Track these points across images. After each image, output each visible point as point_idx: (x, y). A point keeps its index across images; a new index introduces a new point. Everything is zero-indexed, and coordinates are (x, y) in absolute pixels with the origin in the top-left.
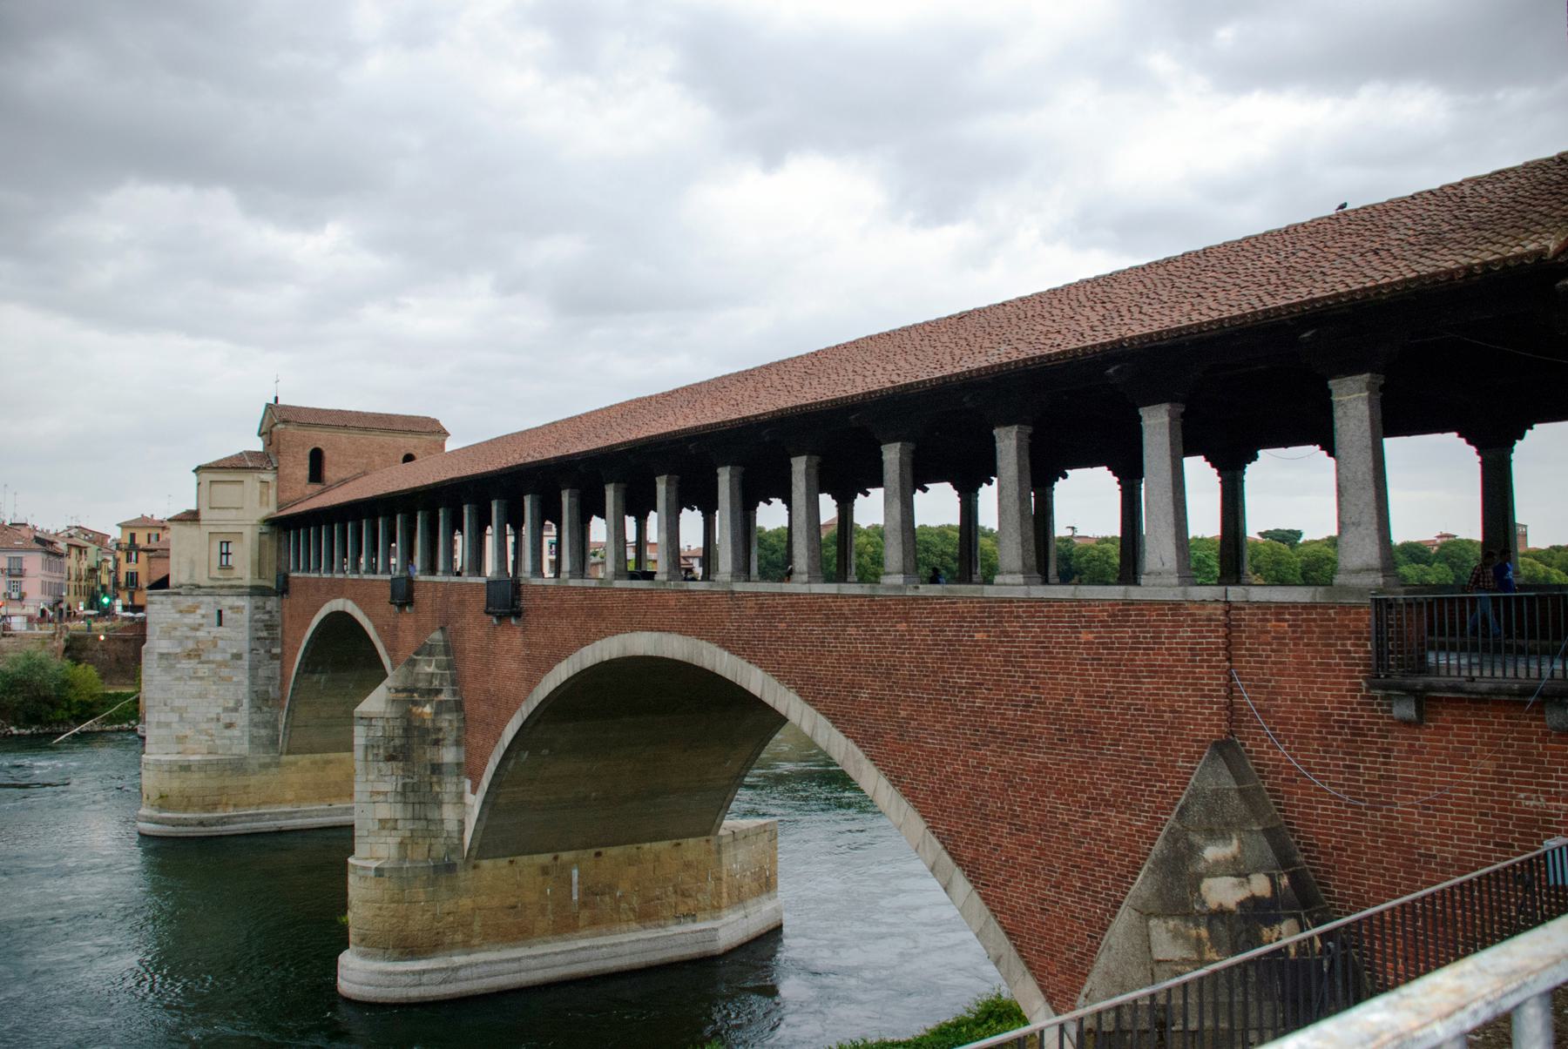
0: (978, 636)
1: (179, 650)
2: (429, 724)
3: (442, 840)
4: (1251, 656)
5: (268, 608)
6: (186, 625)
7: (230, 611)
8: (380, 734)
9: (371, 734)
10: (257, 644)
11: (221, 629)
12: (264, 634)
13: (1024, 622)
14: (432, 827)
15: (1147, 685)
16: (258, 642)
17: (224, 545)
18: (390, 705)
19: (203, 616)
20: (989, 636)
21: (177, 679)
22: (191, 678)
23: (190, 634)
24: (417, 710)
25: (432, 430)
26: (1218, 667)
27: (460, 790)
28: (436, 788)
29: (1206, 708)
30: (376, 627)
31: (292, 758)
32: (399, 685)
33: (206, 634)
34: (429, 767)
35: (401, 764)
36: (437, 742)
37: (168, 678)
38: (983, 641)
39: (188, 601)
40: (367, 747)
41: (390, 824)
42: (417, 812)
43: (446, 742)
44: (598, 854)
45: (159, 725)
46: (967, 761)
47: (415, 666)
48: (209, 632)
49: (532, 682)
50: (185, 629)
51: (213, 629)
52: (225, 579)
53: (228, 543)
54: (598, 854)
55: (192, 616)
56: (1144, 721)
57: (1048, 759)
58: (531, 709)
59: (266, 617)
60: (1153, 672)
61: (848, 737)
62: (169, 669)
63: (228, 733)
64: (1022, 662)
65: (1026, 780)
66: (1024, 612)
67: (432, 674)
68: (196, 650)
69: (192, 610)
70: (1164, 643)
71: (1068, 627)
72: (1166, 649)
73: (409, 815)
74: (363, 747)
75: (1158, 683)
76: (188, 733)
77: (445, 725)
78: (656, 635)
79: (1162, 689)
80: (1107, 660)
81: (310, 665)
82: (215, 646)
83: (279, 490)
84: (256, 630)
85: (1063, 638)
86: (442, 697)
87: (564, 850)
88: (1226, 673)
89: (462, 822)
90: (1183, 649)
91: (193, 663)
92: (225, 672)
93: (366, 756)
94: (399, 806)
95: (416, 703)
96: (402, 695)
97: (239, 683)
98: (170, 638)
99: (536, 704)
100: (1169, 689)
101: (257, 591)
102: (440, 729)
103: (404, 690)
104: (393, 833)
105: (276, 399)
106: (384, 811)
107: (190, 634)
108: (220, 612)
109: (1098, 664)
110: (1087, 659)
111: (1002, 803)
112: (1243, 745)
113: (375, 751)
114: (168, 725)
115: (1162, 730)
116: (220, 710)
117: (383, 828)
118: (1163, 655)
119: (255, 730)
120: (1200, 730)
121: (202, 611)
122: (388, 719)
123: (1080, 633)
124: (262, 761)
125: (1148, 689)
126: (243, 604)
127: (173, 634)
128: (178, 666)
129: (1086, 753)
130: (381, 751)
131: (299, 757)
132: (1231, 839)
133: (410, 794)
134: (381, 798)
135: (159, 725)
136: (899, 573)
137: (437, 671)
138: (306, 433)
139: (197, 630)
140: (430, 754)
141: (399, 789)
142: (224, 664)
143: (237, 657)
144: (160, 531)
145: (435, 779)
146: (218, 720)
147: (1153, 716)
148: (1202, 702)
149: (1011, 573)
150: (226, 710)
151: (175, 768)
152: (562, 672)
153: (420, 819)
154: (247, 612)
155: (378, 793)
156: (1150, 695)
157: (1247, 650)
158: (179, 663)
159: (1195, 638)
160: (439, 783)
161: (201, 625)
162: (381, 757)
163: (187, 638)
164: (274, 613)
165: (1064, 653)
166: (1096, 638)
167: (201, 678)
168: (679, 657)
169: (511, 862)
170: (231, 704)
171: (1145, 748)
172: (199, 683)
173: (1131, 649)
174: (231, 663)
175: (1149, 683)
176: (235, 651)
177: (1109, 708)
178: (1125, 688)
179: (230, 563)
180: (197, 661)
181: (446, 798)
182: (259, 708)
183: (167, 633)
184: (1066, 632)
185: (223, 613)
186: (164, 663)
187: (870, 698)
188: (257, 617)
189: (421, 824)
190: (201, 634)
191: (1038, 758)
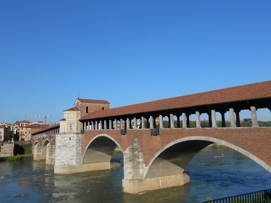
1: (62, 145)
2: (137, 155)
12: (78, 141)
19: (67, 139)
21: (62, 151)
24: (135, 152)
28: (138, 166)
30: (115, 139)
31: (83, 165)
32: (131, 148)
36: (138, 158)
39: (64, 135)
44: (164, 178)
54: (164, 178)
55: (65, 139)
58: (163, 151)
59: (79, 138)
63: (71, 161)
67: (136, 146)
73: (134, 171)
77: (140, 154)
81: (90, 147)
83: (81, 114)
86: (139, 150)
87: (159, 177)
91: (65, 147)
92: (71, 149)
94: (132, 169)
95: (134, 151)
96: (132, 150)
97: (74, 151)
99: (164, 150)
101: (78, 133)
102: (139, 155)
106: (129, 170)
108: (70, 138)
114: (60, 160)
116: (70, 156)
121: (66, 138)
127: (61, 142)
131: (84, 165)
134: (129, 168)
139: (66, 141)
140: (137, 160)
142: (71, 147)
143: (73, 146)
144: (28, 123)
145: (138, 164)
146: (70, 158)
150: (71, 156)
151: (62, 168)
154: (75, 137)
160: (139, 165)
167: (66, 150)
169: (151, 179)
170: (72, 155)
172: (66, 151)
181: (140, 168)
183: (60, 142)
186: (59, 148)
190: (67, 142)
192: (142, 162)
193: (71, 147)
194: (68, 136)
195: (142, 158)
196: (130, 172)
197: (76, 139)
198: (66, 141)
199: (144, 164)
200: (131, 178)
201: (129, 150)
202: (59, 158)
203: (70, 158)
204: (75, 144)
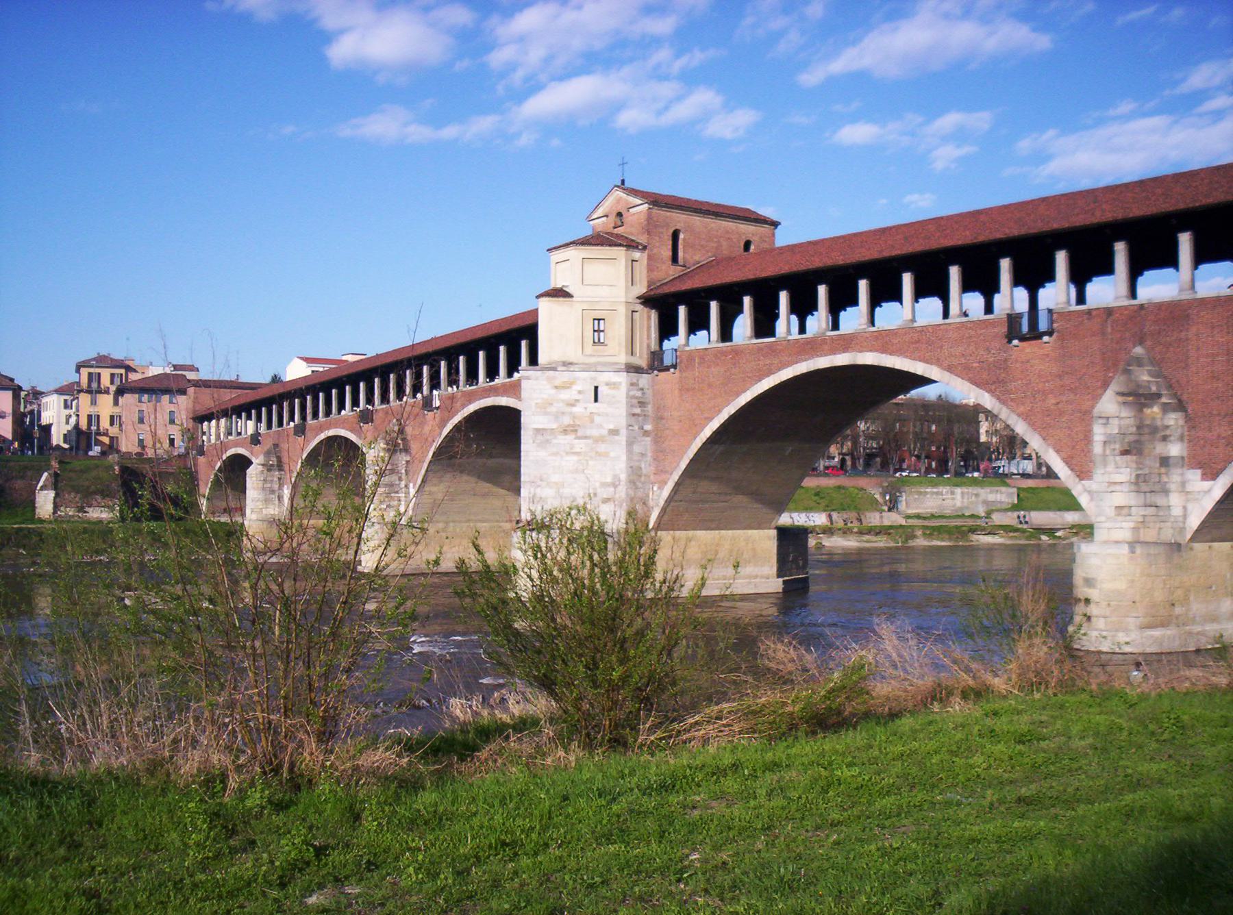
1: (554, 426)
2: (1159, 423)
3: (1169, 524)
5: (641, 386)
6: (563, 401)
8: (1116, 431)
12: (638, 411)
14: (1161, 513)
17: (596, 322)
19: (580, 392)
23: (568, 409)
24: (1148, 411)
28: (1165, 479)
33: (583, 410)
35: (1134, 458)
36: (1165, 439)
39: (562, 377)
41: (1125, 511)
43: (1172, 438)
50: (561, 405)
53: (599, 320)
59: (639, 394)
68: (573, 426)
69: (567, 386)
73: (1141, 501)
74: (1102, 444)
77: (1172, 422)
82: (592, 421)
83: (650, 269)
84: (632, 406)
86: (1164, 400)
92: (602, 448)
93: (1104, 451)
95: (1143, 406)
98: (546, 414)
102: (1167, 427)
104: (1128, 518)
106: (1120, 498)
108: (596, 388)
116: (597, 484)
117: (1119, 515)
128: (555, 441)
133: (1142, 484)
134: (1118, 488)
137: (1150, 379)
138: (668, 214)
139: (573, 405)
140: (1159, 449)
142: (599, 440)
143: (614, 432)
145: (1163, 470)
153: (1150, 506)
154: (624, 388)
155: (1115, 483)
158: (555, 438)
160: (1166, 474)
161: (577, 401)
162: (1117, 452)
163: (563, 413)
164: (645, 391)
169: (1210, 547)
170: (609, 480)
176: (612, 427)
179: (602, 341)
180: (574, 436)
181: (1172, 487)
185: (599, 389)
186: (540, 437)
188: (632, 393)
190: (577, 410)
192: (1183, 458)
193: (599, 440)
195: (1181, 439)
196: (1121, 508)
197: (628, 396)
199: (1192, 466)
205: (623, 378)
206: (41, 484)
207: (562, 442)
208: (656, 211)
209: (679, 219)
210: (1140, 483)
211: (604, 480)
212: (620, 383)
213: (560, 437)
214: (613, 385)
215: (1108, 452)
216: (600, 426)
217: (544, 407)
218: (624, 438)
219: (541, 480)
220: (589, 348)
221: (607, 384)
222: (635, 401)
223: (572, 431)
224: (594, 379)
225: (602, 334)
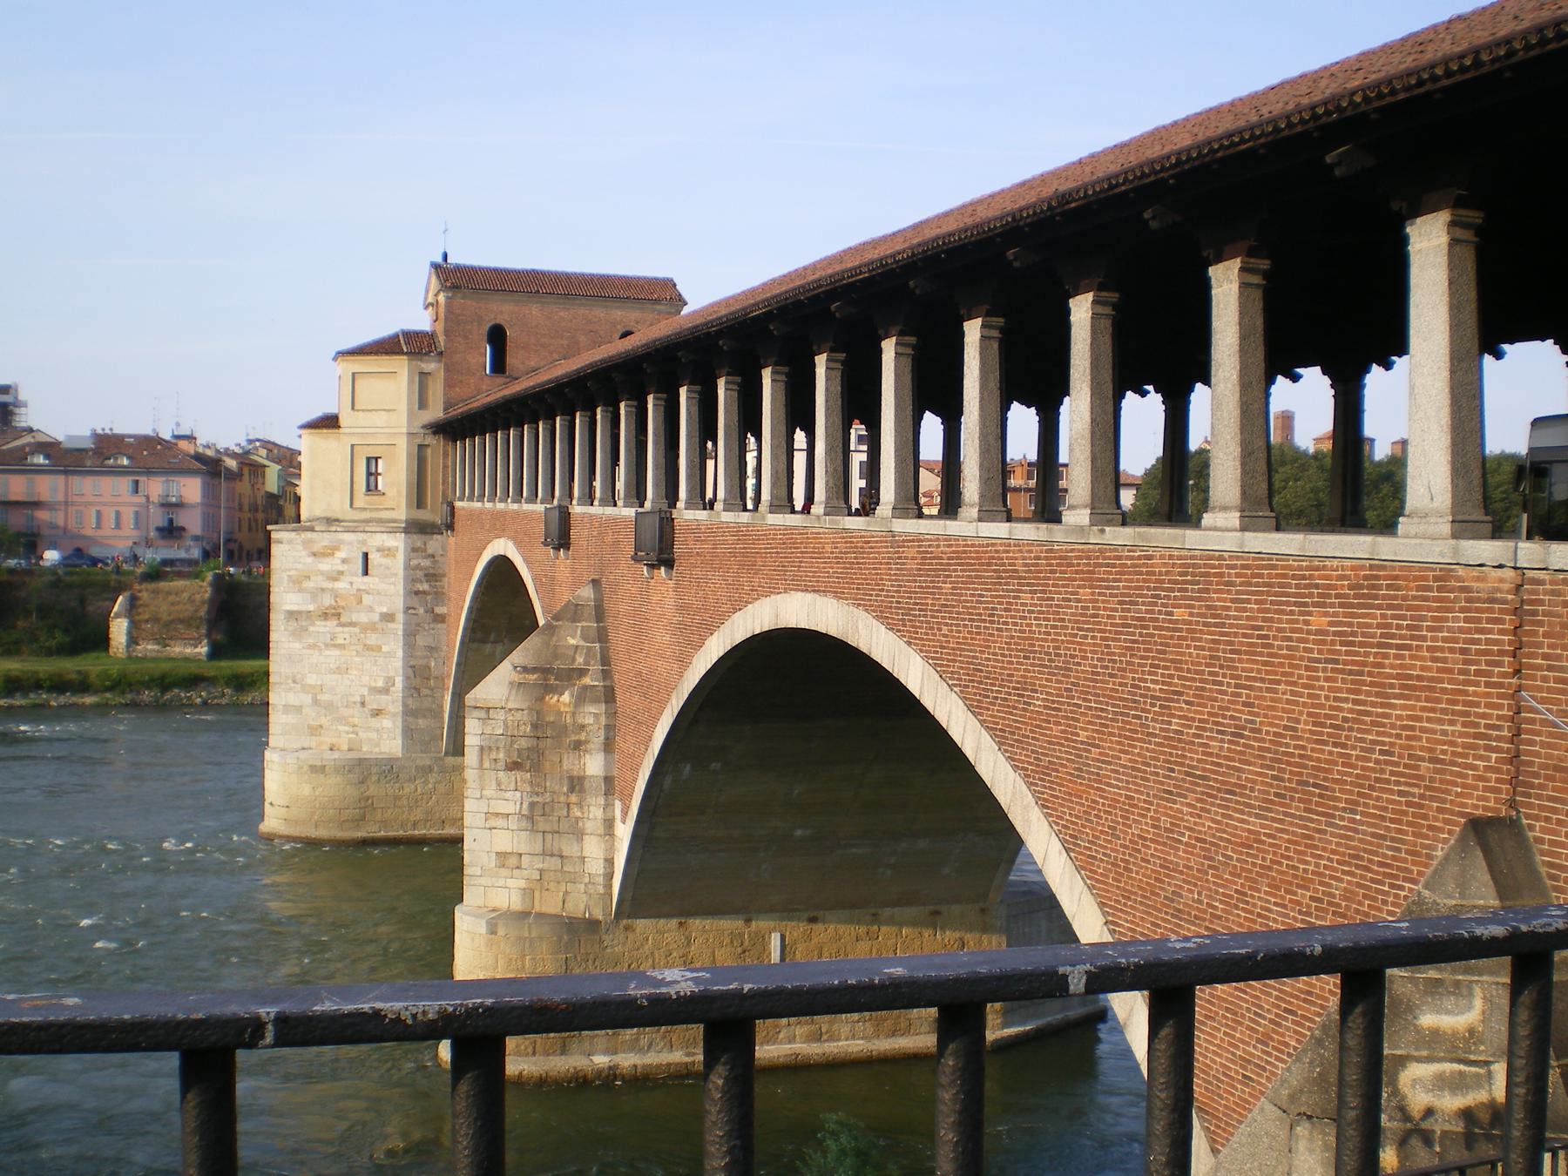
0: (1180, 614)
1: (311, 608)
4: (1550, 668)
5: (430, 551)
6: (322, 573)
7: (378, 554)
9: (488, 730)
10: (415, 601)
11: (366, 579)
12: (425, 587)
13: (1238, 592)
15: (1399, 710)
16: (416, 598)
18: (514, 692)
19: (344, 561)
20: (1191, 614)
21: (310, 647)
22: (327, 646)
23: (330, 585)
24: (552, 699)
25: (662, 293)
26: (1501, 685)
27: (609, 815)
28: (576, 812)
29: (1481, 758)
33: (348, 587)
34: (566, 781)
36: (578, 746)
37: (297, 645)
38: (1185, 622)
39: (322, 540)
40: (482, 749)
41: (513, 861)
42: (548, 845)
45: (288, 708)
46: (1159, 820)
47: (553, 634)
48: (351, 583)
49: (684, 662)
51: (355, 579)
52: (372, 510)
53: (376, 459)
55: (329, 560)
56: (1392, 773)
57: (1262, 826)
59: (426, 563)
60: (1409, 686)
61: (1015, 768)
62: (299, 634)
63: (374, 722)
64: (1233, 660)
65: (1231, 858)
66: (1237, 575)
69: (329, 552)
70: (1424, 639)
71: (1295, 604)
72: (1429, 649)
73: (538, 848)
75: (1413, 708)
76: (323, 721)
77: (590, 720)
78: (809, 597)
79: (1419, 719)
80: (1346, 663)
83: (449, 385)
85: (1288, 621)
86: (587, 681)
88: (1512, 697)
89: (610, 862)
90: (1452, 650)
91: (331, 624)
92: (372, 639)
93: (481, 760)
95: (549, 689)
96: (533, 677)
97: (391, 654)
100: (1429, 720)
102: (582, 727)
103: (534, 670)
104: (516, 872)
105: (445, 257)
106: (505, 840)
107: (330, 585)
108: (366, 556)
109: (1333, 670)
110: (1318, 661)
111: (1199, 894)
112: (1531, 828)
113: (493, 756)
114: (298, 709)
115: (1416, 790)
116: (365, 691)
118: (1422, 659)
119: (410, 719)
120: (1470, 796)
121: (340, 555)
122: (510, 710)
123: (1310, 614)
124: (420, 763)
125: (1399, 717)
126: (396, 544)
128: (311, 629)
129: (1312, 821)
130: (501, 756)
132: (1471, 995)
134: (500, 822)
135: (288, 708)
136: (1086, 507)
137: (582, 643)
139: (335, 579)
140: (569, 763)
141: (525, 811)
142: (370, 628)
143: (388, 617)
145: (573, 798)
147: (1406, 766)
148: (1475, 747)
149: (1225, 508)
151: (305, 768)
152: (715, 648)
153: (552, 855)
155: (497, 815)
156: (1403, 728)
157: (1546, 657)
158: (313, 624)
159: (1469, 631)
160: (580, 805)
161: (342, 573)
162: (501, 765)
163: (323, 590)
165: (1289, 648)
166: (1331, 624)
167: (341, 647)
168: (833, 632)
169: (680, 923)
170: (380, 684)
171: (1392, 821)
172: (337, 652)
173: (1380, 645)
174: (379, 626)
175: (1404, 707)
176: (385, 610)
177: (1344, 746)
178: (1368, 714)
179: (380, 487)
180: (335, 622)
181: (589, 826)
182: (417, 690)
183: (298, 582)
184: (1292, 613)
187: (1045, 707)
188: (414, 562)
189: (554, 863)
190: (341, 585)
191: (1248, 823)
193: (370, 628)
194: (350, 543)
197: (407, 567)
198: (335, 577)
200: (516, 903)
201: (517, 677)
202: (292, 699)
203: (363, 704)
204: (399, 603)
205: (398, 542)
206: (116, 608)
207: (322, 630)
208: (459, 301)
209: (501, 311)
210: (536, 815)
211: (373, 684)
212: (397, 548)
213: (318, 623)
214: (386, 552)
215: (486, 764)
216: (371, 609)
217: (298, 582)
218: (401, 626)
219: (294, 682)
220: (361, 499)
221: (379, 550)
222: (419, 574)
223: (333, 615)
224: (364, 542)
225: (380, 478)
